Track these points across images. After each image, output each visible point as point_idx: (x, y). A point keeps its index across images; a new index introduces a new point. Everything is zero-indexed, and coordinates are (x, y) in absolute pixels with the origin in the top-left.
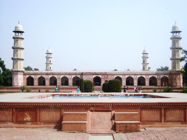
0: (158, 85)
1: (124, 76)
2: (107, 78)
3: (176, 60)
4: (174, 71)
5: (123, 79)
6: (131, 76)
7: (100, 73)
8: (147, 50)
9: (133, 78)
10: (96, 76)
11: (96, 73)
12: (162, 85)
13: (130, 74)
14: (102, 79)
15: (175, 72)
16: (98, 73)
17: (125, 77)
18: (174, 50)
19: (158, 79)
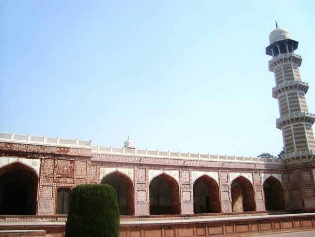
0: (257, 210)
1: (141, 172)
2: (71, 174)
3: (304, 123)
4: (298, 158)
5: (137, 187)
6: (167, 172)
7: (32, 149)
8: (132, 142)
9: (177, 179)
10: (12, 160)
11: (15, 148)
12: (234, 213)
13: (167, 163)
14: (42, 181)
15: (304, 161)
16: (23, 149)
17: (146, 176)
18: (292, 94)
19: (255, 187)
